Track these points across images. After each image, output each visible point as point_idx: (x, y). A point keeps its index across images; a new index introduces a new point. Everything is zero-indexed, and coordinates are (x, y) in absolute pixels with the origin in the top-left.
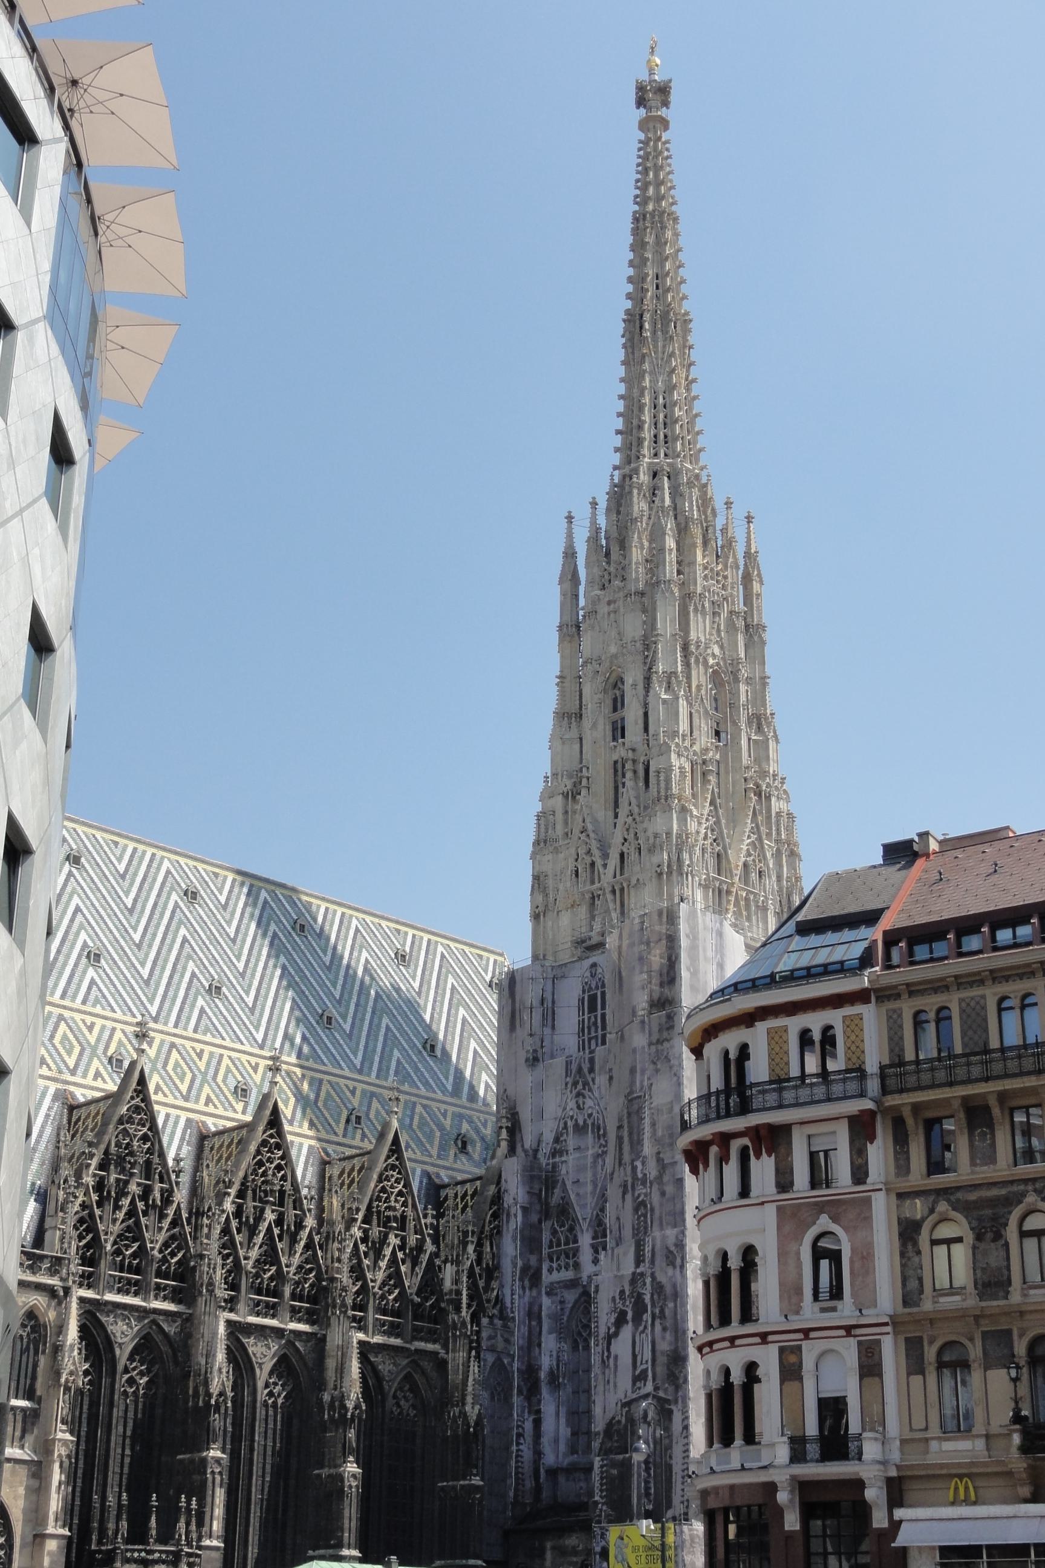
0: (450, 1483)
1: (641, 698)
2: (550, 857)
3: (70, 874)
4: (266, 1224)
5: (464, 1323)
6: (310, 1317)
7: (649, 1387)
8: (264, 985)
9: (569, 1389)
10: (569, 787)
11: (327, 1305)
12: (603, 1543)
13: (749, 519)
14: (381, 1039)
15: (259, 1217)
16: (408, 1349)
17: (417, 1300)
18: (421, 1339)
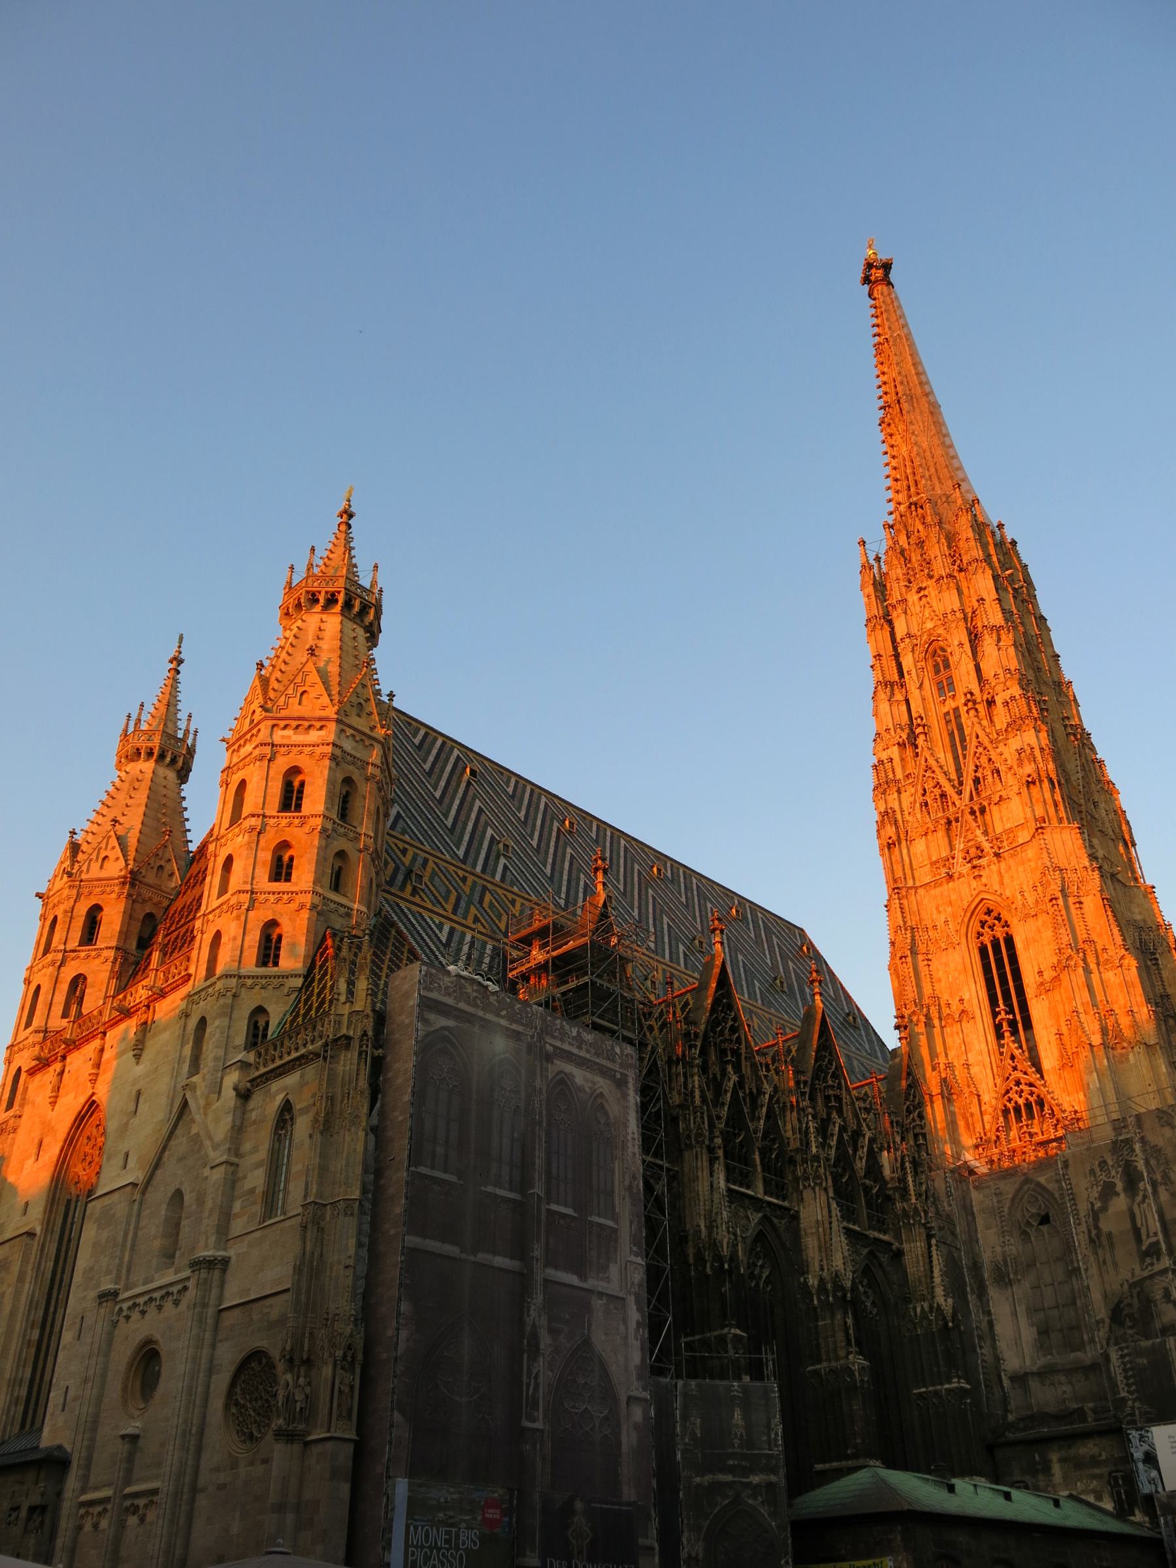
0: (931, 1389)
1: (970, 654)
2: (896, 795)
3: (469, 784)
4: (731, 1084)
5: (916, 1209)
6: (779, 1192)
7: (1166, 1262)
8: (643, 907)
9: (1026, 1285)
10: (905, 736)
11: (796, 1180)
12: (1146, 1447)
13: (1014, 543)
14: (742, 970)
15: (724, 1072)
16: (867, 1236)
17: (867, 1182)
18: (874, 1229)
